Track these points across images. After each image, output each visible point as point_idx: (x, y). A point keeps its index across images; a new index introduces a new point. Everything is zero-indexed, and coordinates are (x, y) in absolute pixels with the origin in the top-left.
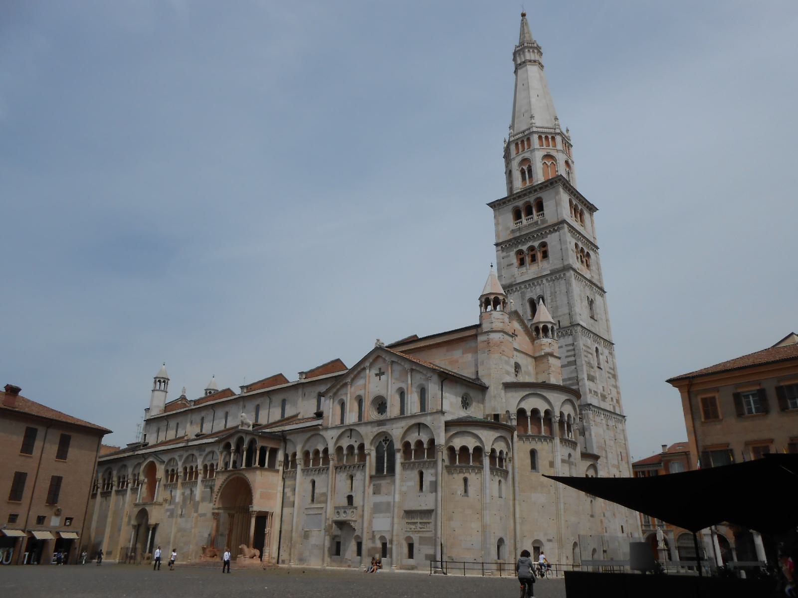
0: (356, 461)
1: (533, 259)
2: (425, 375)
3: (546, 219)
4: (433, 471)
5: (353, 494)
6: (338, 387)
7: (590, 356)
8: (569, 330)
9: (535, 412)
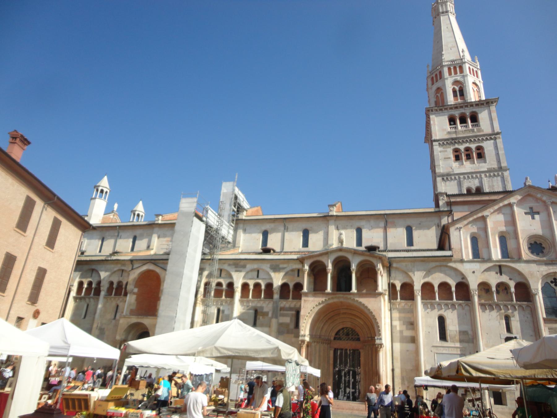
1: (469, 157)
3: (482, 128)
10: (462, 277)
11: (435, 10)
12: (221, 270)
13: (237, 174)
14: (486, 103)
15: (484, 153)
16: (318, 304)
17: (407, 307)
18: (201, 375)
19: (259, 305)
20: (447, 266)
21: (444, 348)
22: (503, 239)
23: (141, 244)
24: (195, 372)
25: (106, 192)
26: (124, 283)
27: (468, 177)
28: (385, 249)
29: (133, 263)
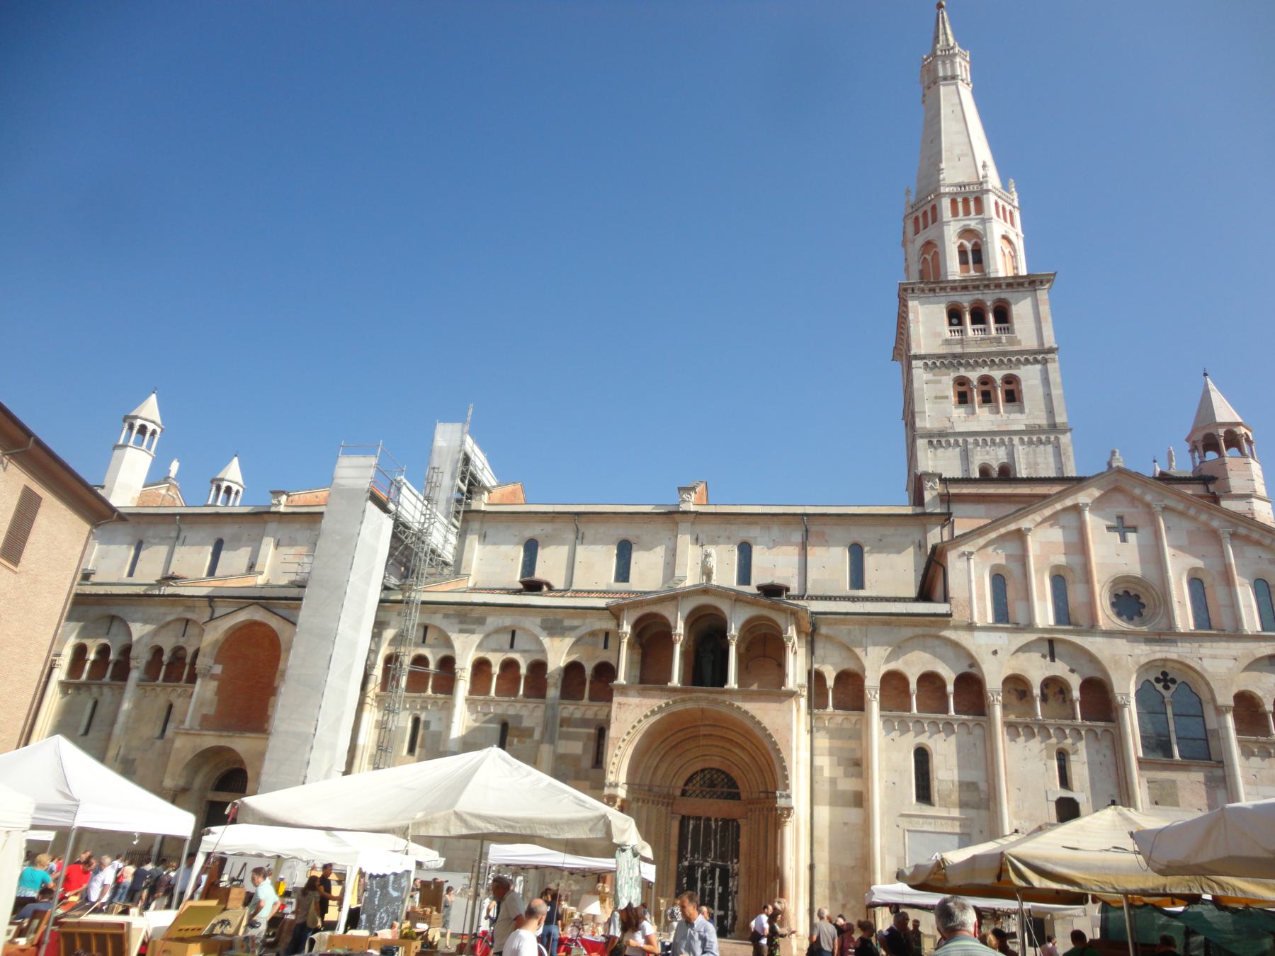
0: (1079, 716)
1: (987, 398)
3: (1019, 338)
10: (970, 662)
11: (928, 70)
12: (426, 628)
13: (472, 405)
14: (1029, 283)
15: (1020, 392)
16: (649, 714)
17: (846, 725)
18: (385, 876)
19: (511, 711)
20: (938, 637)
21: (925, 820)
22: (1059, 581)
23: (233, 560)
24: (369, 870)
25: (154, 433)
26: (190, 651)
27: (985, 441)
28: (801, 594)
29: (212, 604)
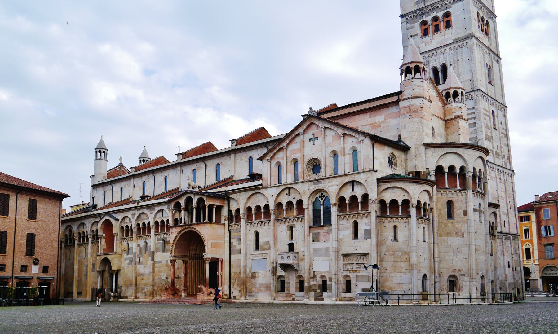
0: (295, 214)
1: (437, 29)
2: (357, 139)
4: (365, 220)
5: (294, 242)
6: (275, 151)
7: (487, 118)
8: (470, 95)
9: (452, 168)
19: (165, 237)
